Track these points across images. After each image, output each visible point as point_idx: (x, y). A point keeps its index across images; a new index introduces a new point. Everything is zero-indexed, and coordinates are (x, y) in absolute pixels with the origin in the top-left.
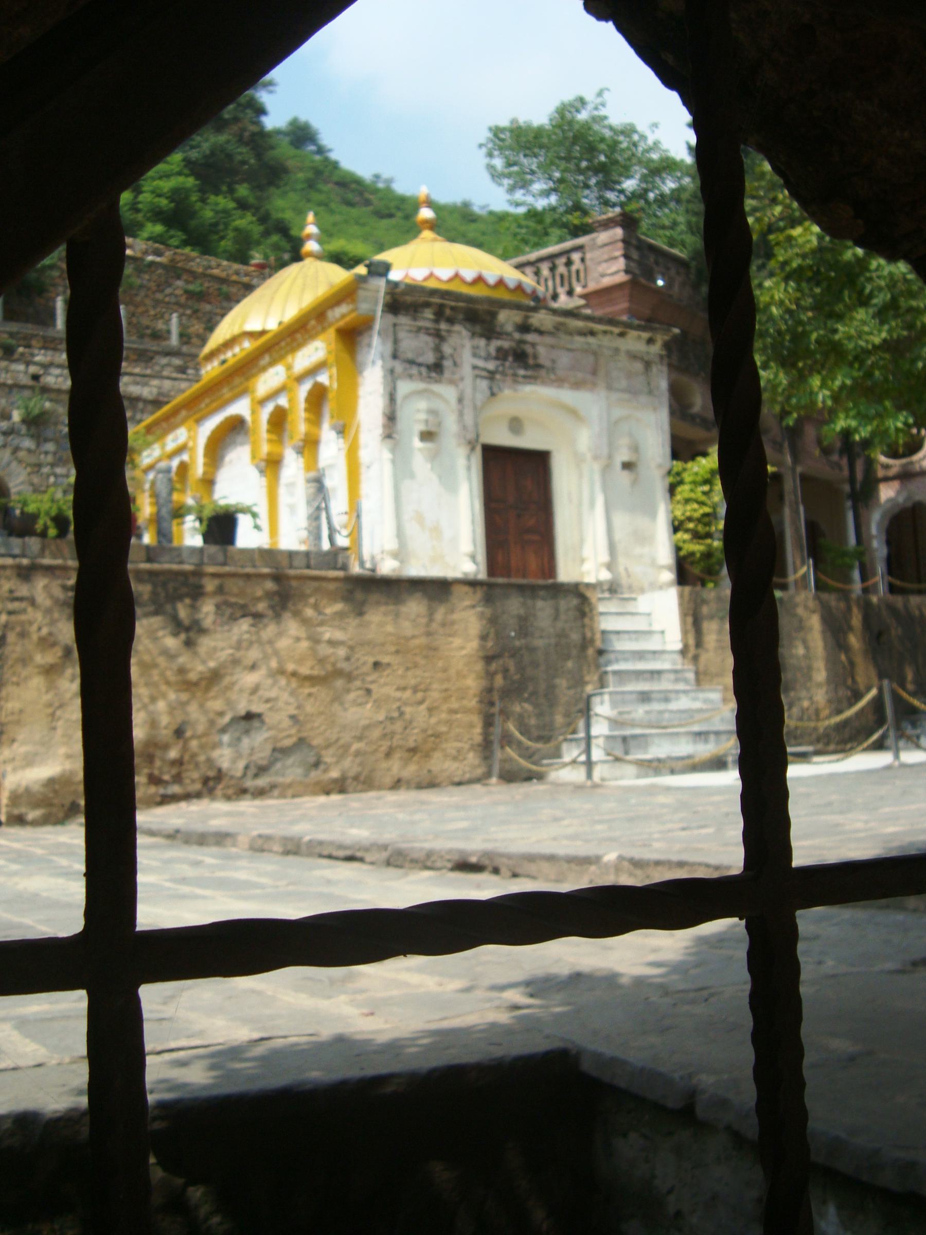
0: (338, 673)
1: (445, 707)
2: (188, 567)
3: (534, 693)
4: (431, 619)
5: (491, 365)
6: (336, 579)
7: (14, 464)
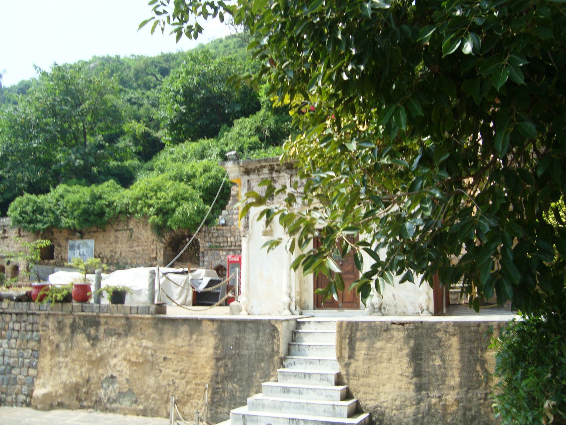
0: (146, 361)
1: (194, 382)
2: (95, 314)
3: (240, 379)
4: (191, 339)
6: (148, 319)
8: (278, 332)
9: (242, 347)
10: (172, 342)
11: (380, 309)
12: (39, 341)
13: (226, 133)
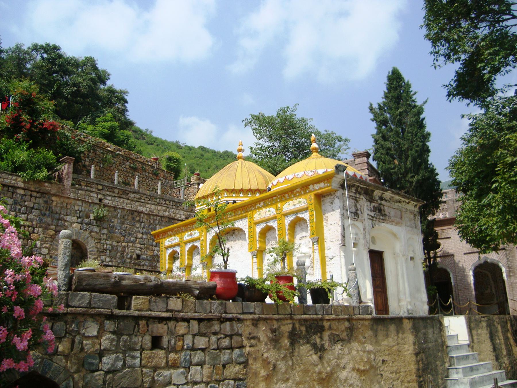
1: (406, 380)
5: (372, 214)
6: (368, 319)
7: (90, 238)
10: (386, 343)
12: (245, 364)
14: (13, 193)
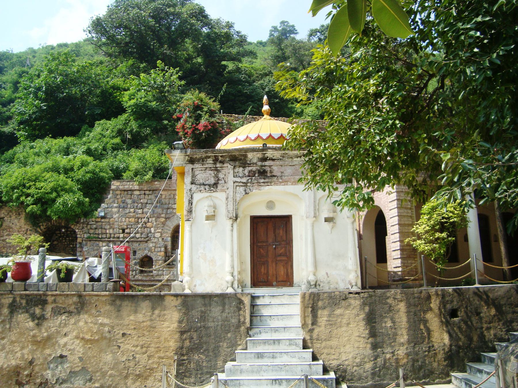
0: (103, 338)
2: (41, 292)
4: (153, 314)
8: (244, 304)
9: (208, 320)
10: (132, 318)
11: (315, 285)
13: (87, 133)
14: (131, 195)
